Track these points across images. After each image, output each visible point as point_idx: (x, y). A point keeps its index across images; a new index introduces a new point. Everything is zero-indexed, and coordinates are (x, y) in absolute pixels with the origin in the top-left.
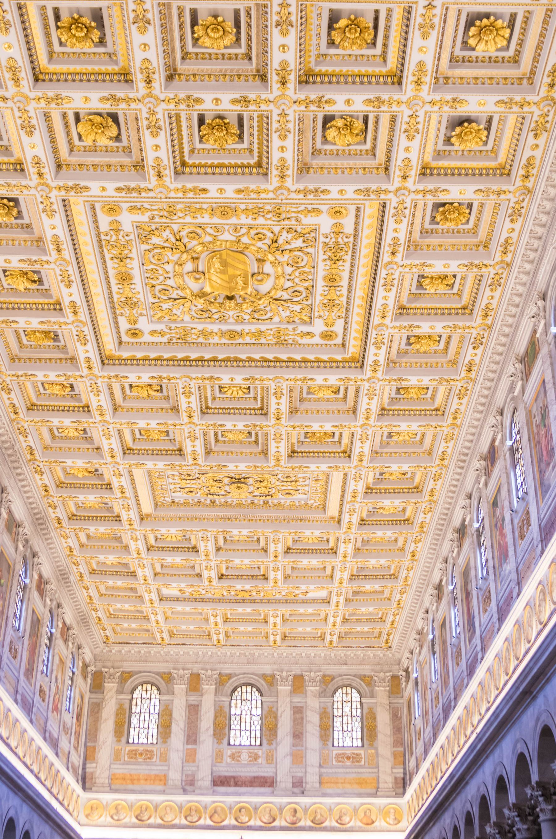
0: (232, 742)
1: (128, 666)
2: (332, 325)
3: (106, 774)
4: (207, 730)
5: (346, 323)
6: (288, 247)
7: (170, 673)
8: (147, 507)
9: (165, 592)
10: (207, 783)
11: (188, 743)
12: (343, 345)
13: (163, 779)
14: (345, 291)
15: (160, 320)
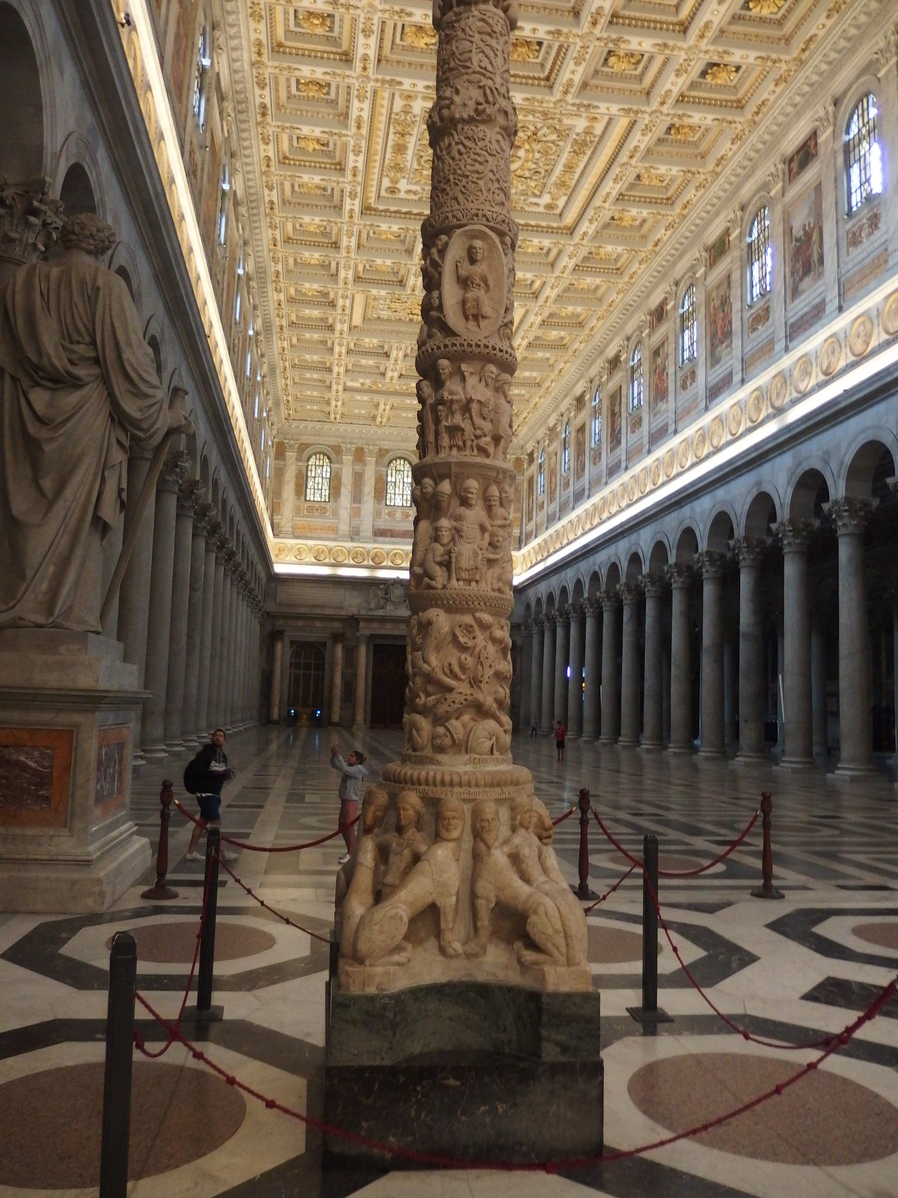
0: (388, 503)
1: (305, 439)
2: (557, 199)
3: (290, 524)
4: (370, 493)
5: (569, 199)
6: (544, 139)
7: (339, 446)
8: (357, 320)
9: (350, 384)
10: (370, 533)
11: (354, 503)
12: (561, 215)
13: (335, 529)
14: (576, 176)
15: (417, 183)
